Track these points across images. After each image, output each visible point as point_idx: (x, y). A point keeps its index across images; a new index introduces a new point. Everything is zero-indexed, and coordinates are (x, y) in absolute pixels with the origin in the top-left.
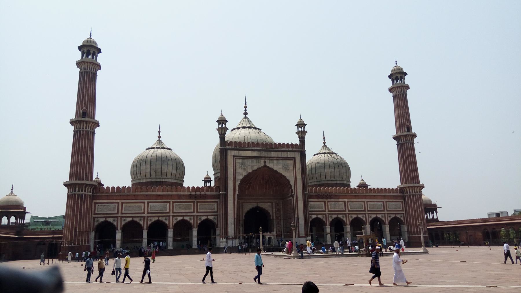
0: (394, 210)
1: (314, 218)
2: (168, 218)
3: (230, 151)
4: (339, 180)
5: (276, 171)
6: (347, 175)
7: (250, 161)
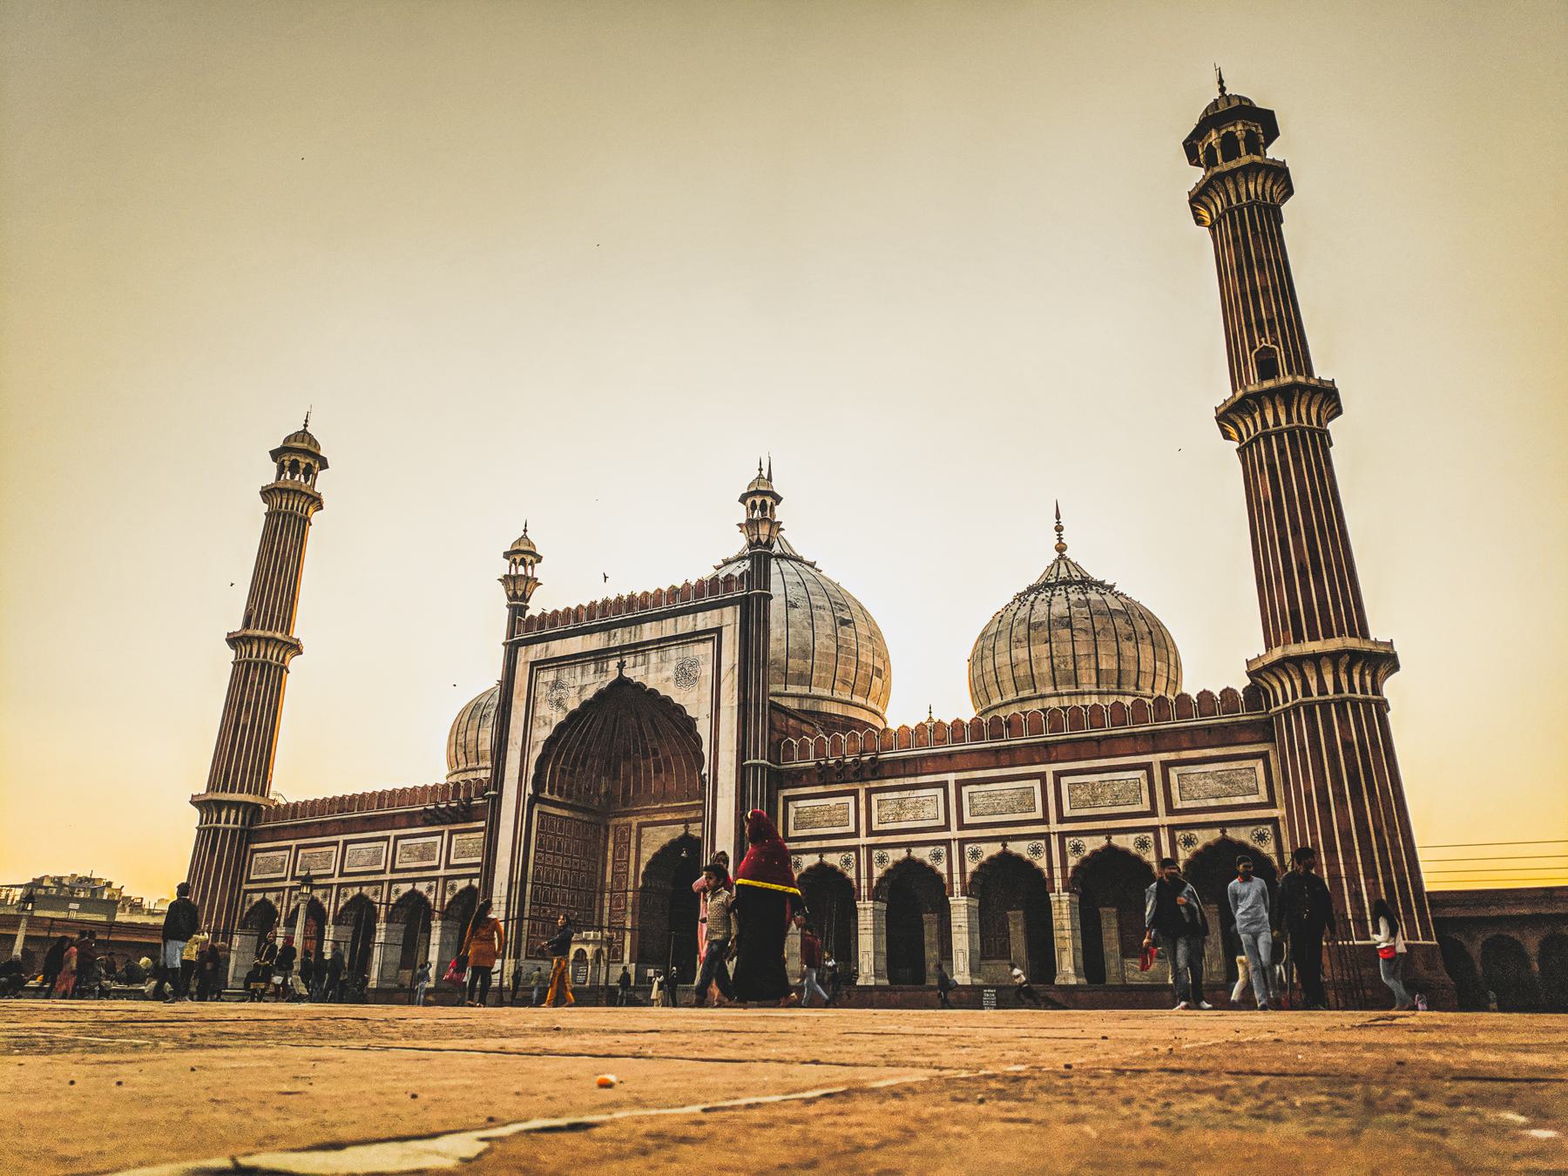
0: (1213, 803)
1: (809, 869)
4: (1051, 696)
5: (653, 692)
6: (1103, 666)
7: (579, 670)
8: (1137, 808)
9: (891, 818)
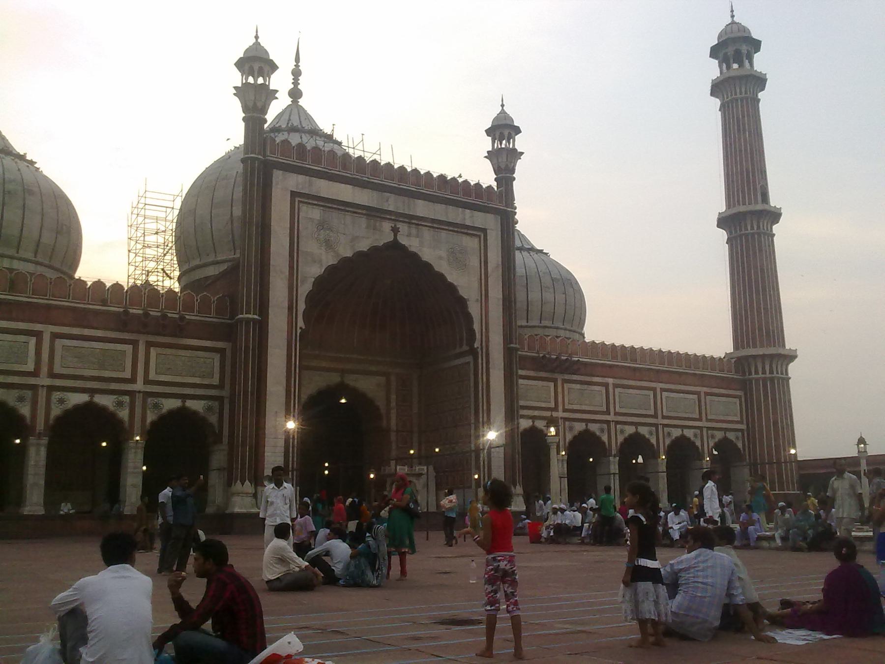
0: (722, 418)
1: (525, 430)
2: (29, 394)
3: (281, 172)
4: (561, 329)
5: (428, 266)
7: (348, 218)
8: (694, 416)
9: (576, 402)
